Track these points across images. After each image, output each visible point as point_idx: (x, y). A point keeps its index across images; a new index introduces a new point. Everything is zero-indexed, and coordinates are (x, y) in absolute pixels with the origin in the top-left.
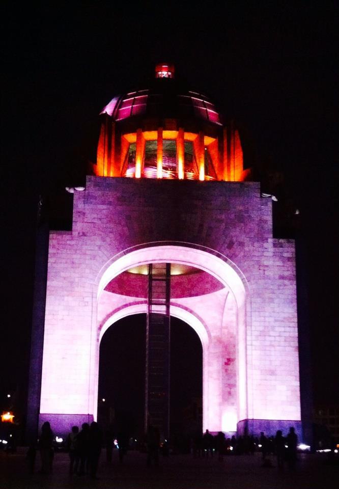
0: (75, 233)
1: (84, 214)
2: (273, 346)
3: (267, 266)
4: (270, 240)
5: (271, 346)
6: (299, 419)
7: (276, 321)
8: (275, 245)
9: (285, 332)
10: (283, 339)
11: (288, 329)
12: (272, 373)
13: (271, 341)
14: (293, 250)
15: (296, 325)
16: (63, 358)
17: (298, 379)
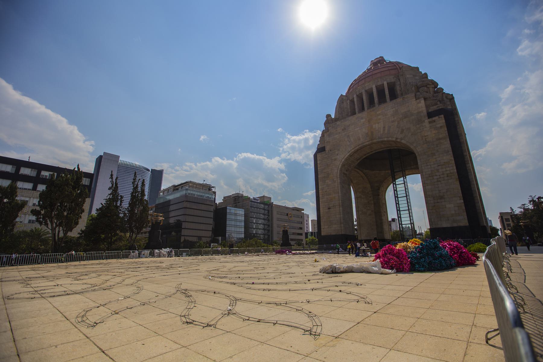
0: (327, 152)
1: (330, 141)
2: (440, 181)
3: (427, 136)
4: (427, 121)
5: (438, 181)
6: (467, 224)
7: (439, 166)
8: (430, 122)
9: (446, 171)
10: (446, 175)
11: (448, 169)
12: (442, 198)
13: (437, 179)
14: (444, 121)
15: (454, 165)
16: (329, 208)
17: (462, 198)
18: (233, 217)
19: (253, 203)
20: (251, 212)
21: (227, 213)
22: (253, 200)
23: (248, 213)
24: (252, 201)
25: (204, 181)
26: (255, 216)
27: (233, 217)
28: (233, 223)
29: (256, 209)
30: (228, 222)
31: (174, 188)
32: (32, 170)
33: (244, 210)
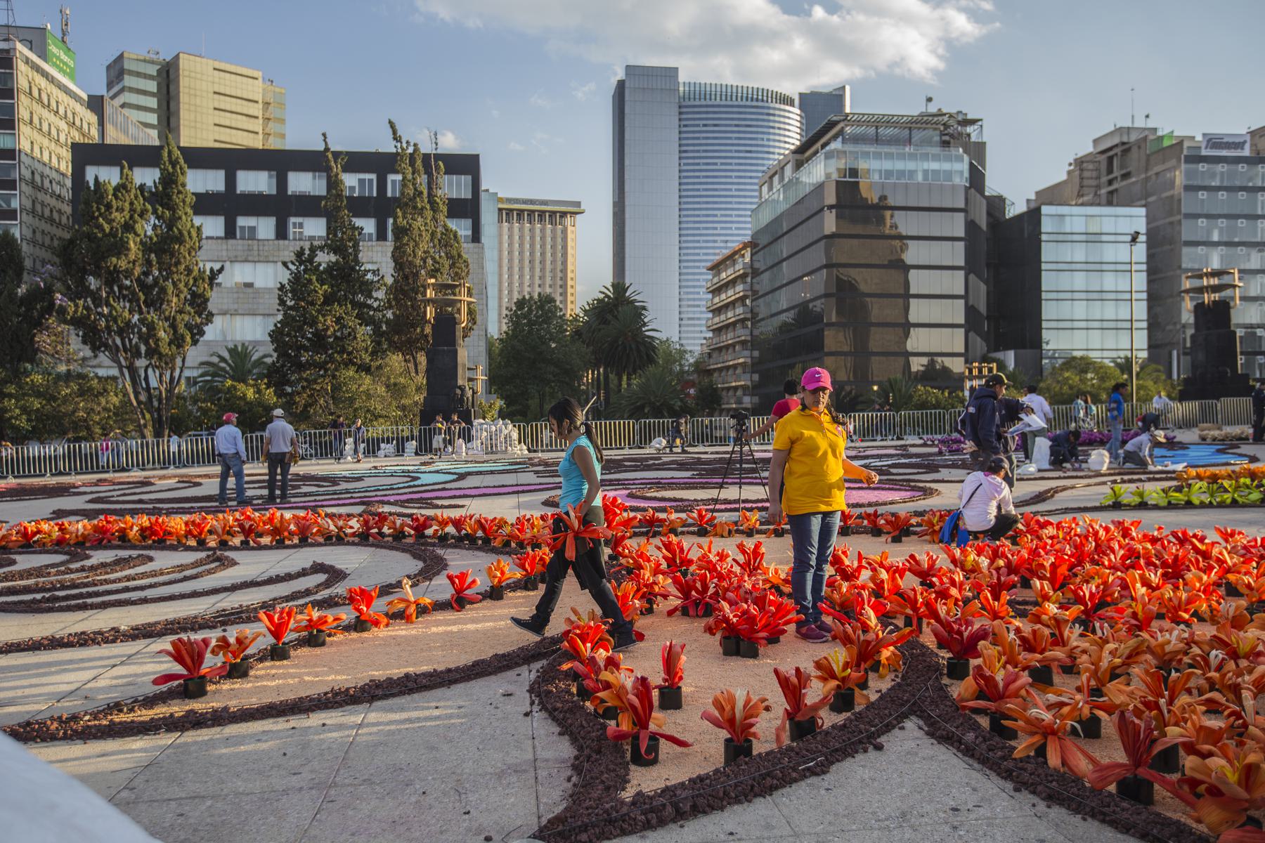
18: (1079, 253)
19: (1202, 167)
20: (1188, 216)
21: (1044, 237)
22: (1204, 153)
23: (1172, 223)
24: (1195, 159)
25: (929, 100)
26: (1221, 234)
27: (1079, 253)
28: (1079, 281)
29: (1222, 195)
30: (1048, 281)
31: (798, 157)
32: (314, 178)
33: (1143, 211)
